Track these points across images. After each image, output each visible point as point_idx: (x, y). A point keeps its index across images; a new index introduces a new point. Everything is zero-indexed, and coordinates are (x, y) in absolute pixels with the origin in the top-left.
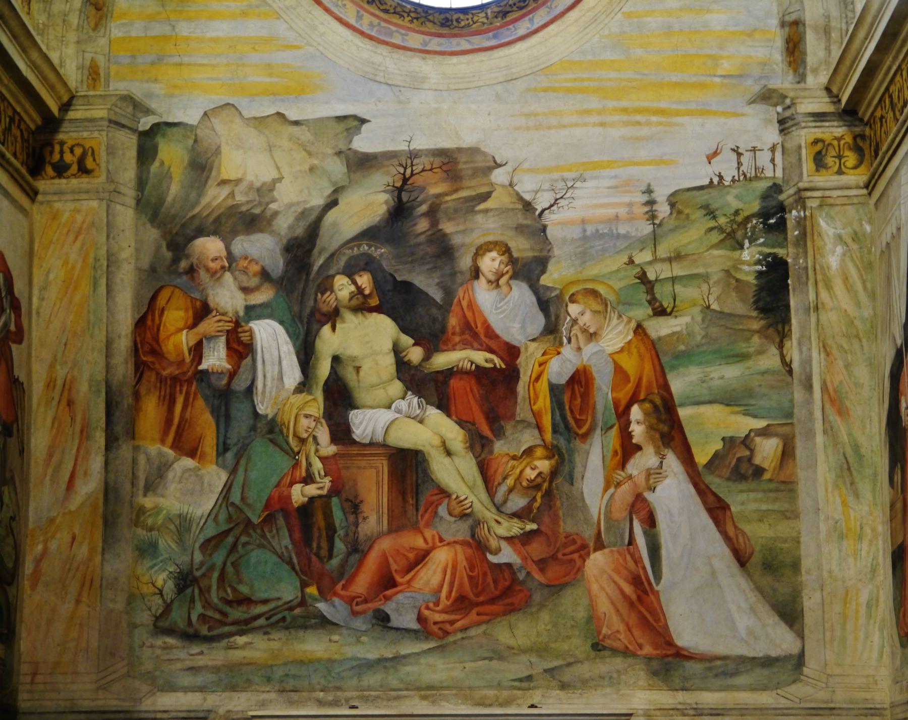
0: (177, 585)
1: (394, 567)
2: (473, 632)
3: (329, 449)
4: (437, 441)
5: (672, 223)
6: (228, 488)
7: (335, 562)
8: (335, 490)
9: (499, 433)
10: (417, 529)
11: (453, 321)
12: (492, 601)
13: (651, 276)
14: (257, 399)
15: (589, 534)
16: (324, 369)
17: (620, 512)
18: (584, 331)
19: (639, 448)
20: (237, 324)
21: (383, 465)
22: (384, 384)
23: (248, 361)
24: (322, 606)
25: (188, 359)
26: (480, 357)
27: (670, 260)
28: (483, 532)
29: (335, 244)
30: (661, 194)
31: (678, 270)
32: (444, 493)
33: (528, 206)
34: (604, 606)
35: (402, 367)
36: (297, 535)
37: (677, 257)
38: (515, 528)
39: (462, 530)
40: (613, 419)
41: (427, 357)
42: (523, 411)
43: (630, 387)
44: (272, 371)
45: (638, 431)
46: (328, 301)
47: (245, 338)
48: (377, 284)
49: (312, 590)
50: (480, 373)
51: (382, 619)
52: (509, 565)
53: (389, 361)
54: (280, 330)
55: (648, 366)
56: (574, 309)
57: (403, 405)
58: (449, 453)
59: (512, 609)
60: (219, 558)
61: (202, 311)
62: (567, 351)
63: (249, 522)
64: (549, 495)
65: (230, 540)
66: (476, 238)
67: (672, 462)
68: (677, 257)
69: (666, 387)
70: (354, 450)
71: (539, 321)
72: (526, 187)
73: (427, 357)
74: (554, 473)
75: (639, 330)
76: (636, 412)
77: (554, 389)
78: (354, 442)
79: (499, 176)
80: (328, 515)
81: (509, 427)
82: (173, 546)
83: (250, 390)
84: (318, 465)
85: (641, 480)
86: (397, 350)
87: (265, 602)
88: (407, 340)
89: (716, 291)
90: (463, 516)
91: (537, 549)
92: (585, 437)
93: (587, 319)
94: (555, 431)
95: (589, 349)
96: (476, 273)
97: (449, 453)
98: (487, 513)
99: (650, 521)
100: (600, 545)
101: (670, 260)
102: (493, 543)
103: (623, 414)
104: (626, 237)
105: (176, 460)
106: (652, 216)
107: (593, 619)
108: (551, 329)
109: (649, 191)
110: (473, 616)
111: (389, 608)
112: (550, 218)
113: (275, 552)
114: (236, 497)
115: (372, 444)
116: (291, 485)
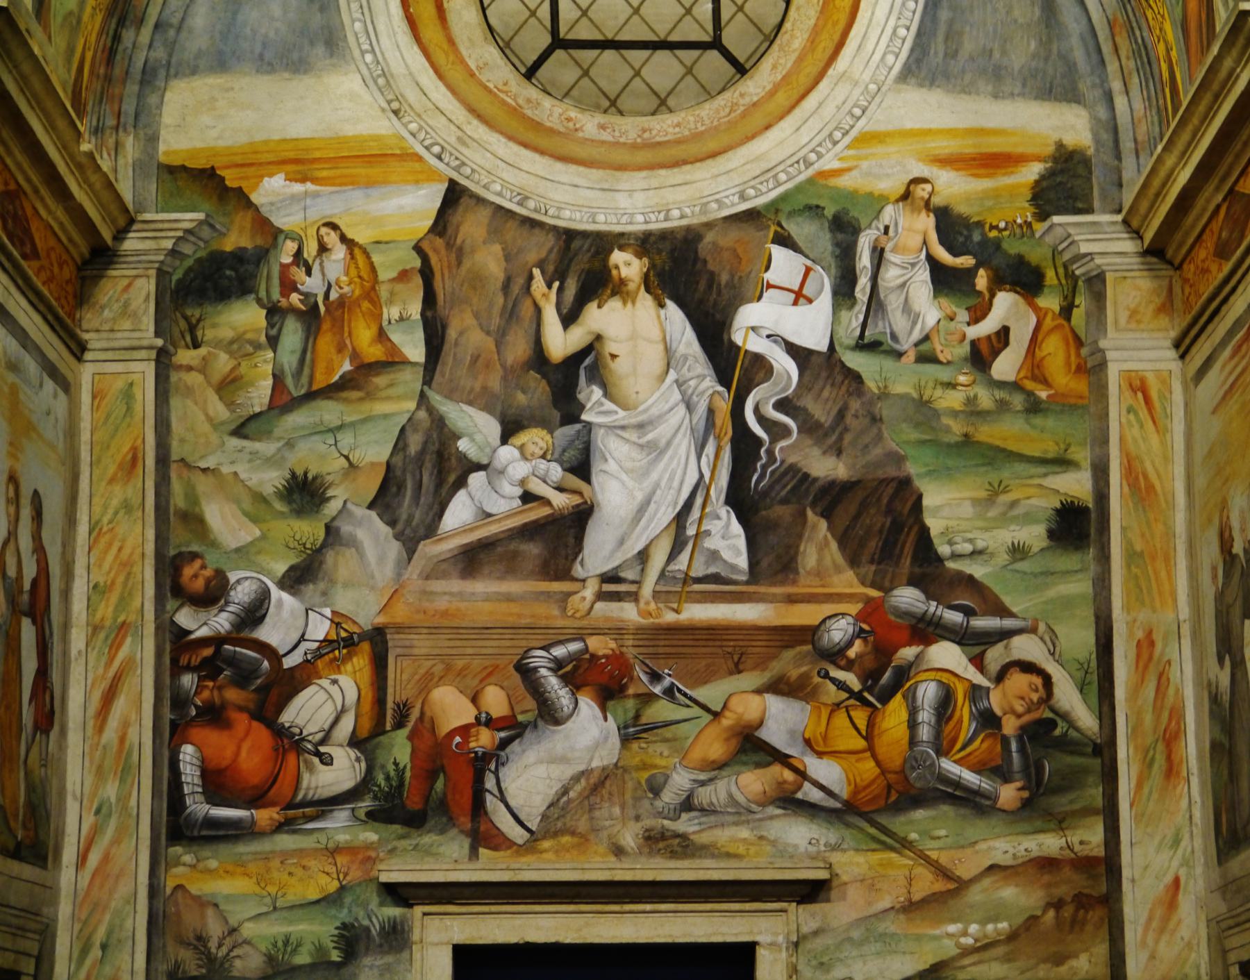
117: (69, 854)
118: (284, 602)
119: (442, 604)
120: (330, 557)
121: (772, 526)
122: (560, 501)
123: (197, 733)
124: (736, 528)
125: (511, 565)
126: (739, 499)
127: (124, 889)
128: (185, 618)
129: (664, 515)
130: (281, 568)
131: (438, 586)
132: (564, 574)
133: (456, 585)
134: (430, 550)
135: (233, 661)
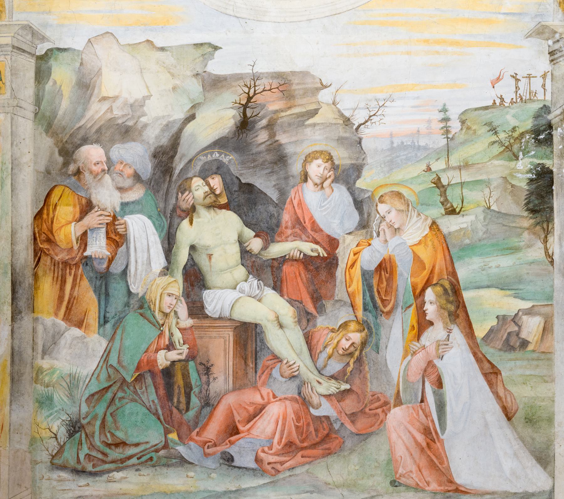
0: (68, 431)
1: (237, 418)
2: (298, 471)
3: (187, 322)
4: (272, 317)
5: (462, 137)
6: (107, 353)
7: (191, 414)
8: (192, 356)
9: (321, 310)
10: (255, 387)
11: (286, 217)
12: (314, 446)
13: (445, 182)
14: (131, 280)
18: (390, 226)
19: (431, 323)
20: (115, 218)
21: (229, 335)
23: (123, 249)
24: (181, 449)
25: (76, 247)
26: (308, 248)
27: (460, 168)
28: (307, 391)
29: (192, 153)
30: (454, 113)
31: (466, 176)
32: (277, 359)
33: (347, 121)
34: (401, 451)
36: (162, 392)
37: (465, 166)
38: (332, 387)
39: (290, 390)
40: (412, 300)
41: (265, 248)
43: (425, 274)
44: (142, 257)
45: (431, 310)
46: (186, 201)
47: (120, 229)
48: (226, 186)
49: (173, 436)
51: (228, 459)
52: (327, 418)
54: (149, 223)
55: (440, 256)
56: (382, 208)
57: (245, 286)
58: (281, 326)
59: (329, 453)
60: (100, 409)
62: (376, 243)
63: (124, 380)
64: (359, 360)
65: (109, 395)
66: (306, 148)
67: (457, 335)
68: (465, 166)
69: (454, 274)
70: (206, 323)
71: (356, 217)
72: (346, 107)
73: (265, 248)
74: (364, 344)
75: (434, 225)
76: (430, 294)
77: (365, 274)
78: (207, 317)
79: (325, 96)
80: (186, 376)
81: (329, 305)
82: (65, 399)
83: (125, 273)
84: (178, 335)
85: (432, 350)
87: (137, 445)
89: (496, 194)
90: (293, 377)
91: (350, 405)
92: (389, 313)
93: (392, 217)
94: (365, 309)
95: (394, 242)
96: (305, 177)
97: (281, 326)
98: (310, 375)
101: (460, 168)
102: (315, 400)
103: (419, 295)
104: (425, 148)
105: (67, 330)
106: (447, 131)
107: (392, 461)
108: (364, 225)
109: (444, 110)
110: (298, 458)
111: (233, 451)
112: (365, 132)
113: (144, 405)
114: (113, 361)
115: (220, 318)
116: (157, 351)
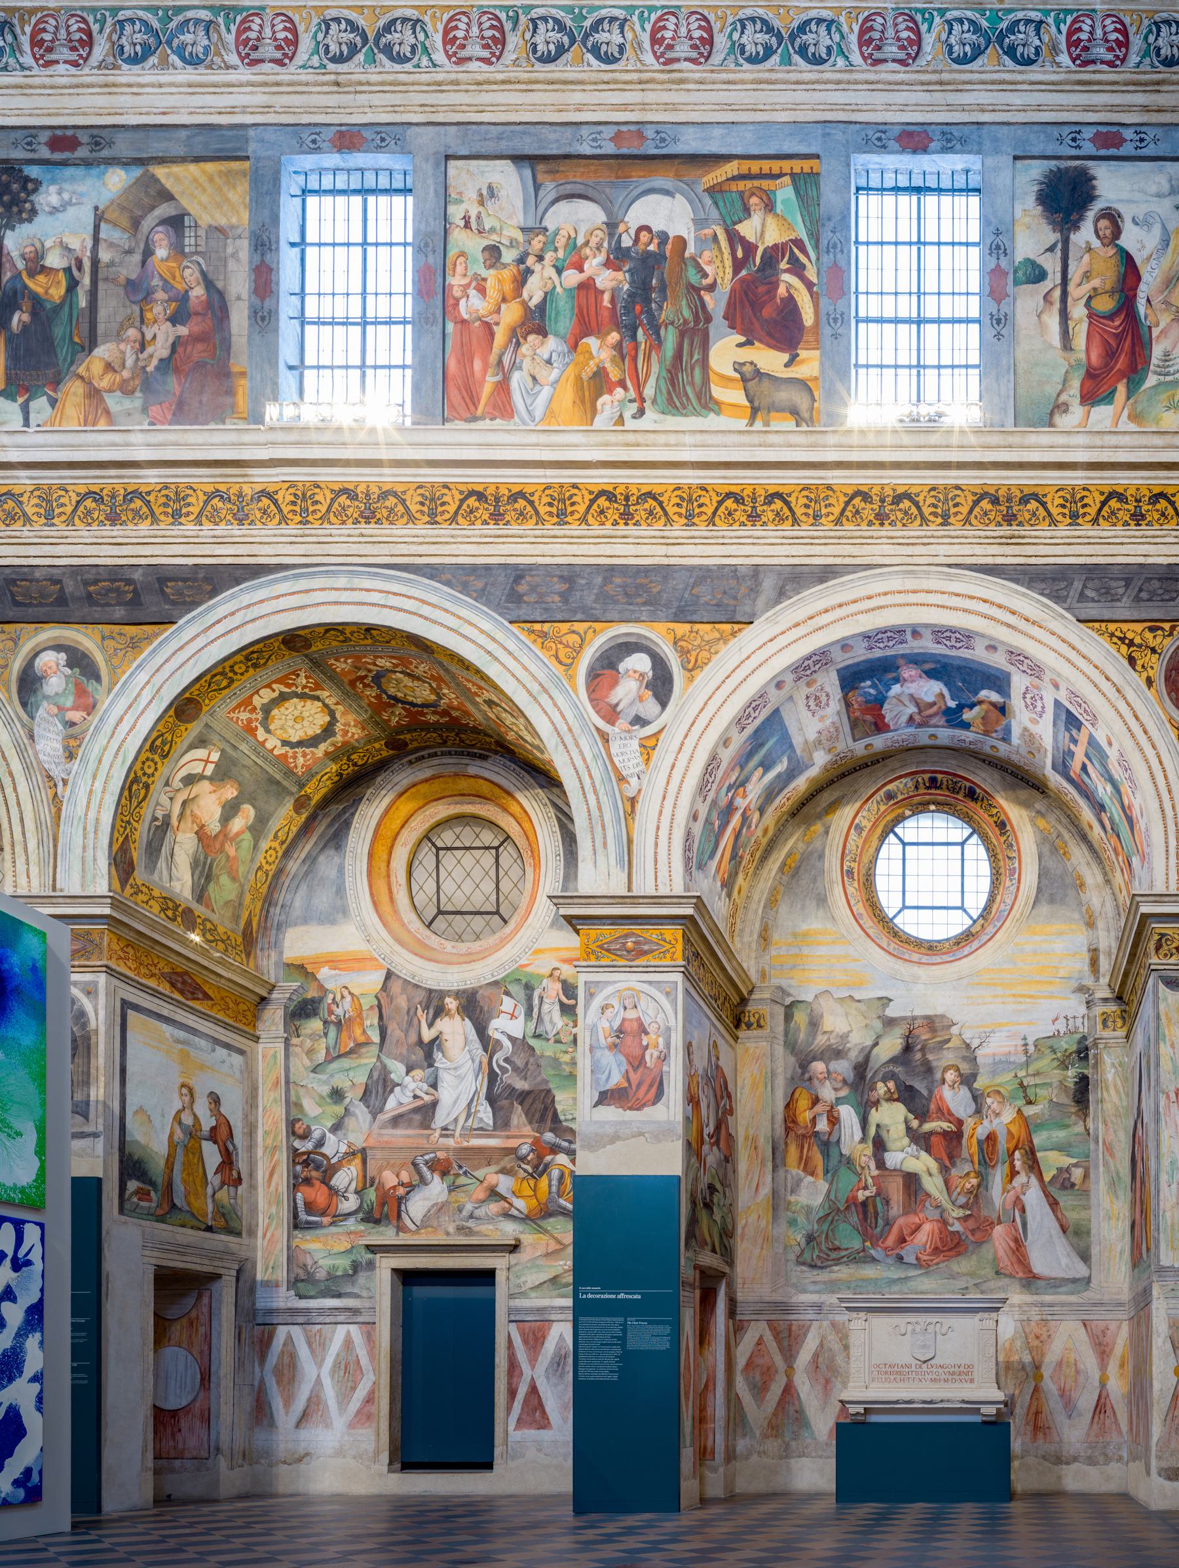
9: (953, 1164)
15: (994, 1217)
16: (872, 1131)
17: (1009, 1206)
22: (900, 1139)
35: (909, 1129)
42: (965, 1154)
50: (945, 1134)
53: (902, 1127)
61: (816, 1101)
81: (958, 1161)
86: (906, 1122)
88: (911, 1116)
99: (1023, 1210)
100: (1000, 1222)
117: (260, 1234)
118: (331, 1138)
119: (386, 1138)
120: (346, 1120)
121: (502, 1108)
122: (427, 1098)
123: (302, 1188)
124: (489, 1109)
125: (410, 1125)
126: (491, 1099)
127: (279, 1247)
128: (297, 1144)
129: (463, 1104)
130: (329, 1125)
131: (384, 1131)
132: (428, 1127)
133: (390, 1131)
134: (382, 1117)
135: (313, 1161)
